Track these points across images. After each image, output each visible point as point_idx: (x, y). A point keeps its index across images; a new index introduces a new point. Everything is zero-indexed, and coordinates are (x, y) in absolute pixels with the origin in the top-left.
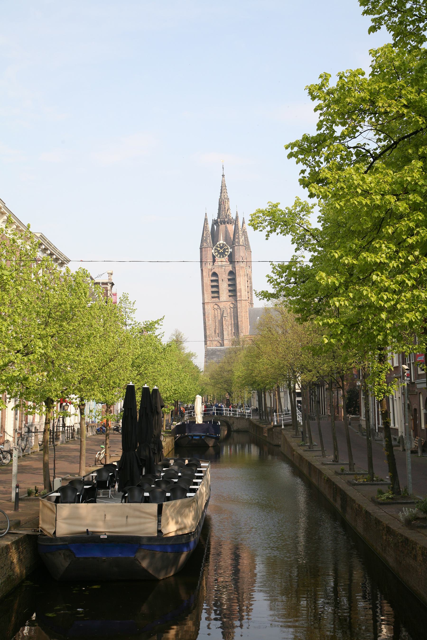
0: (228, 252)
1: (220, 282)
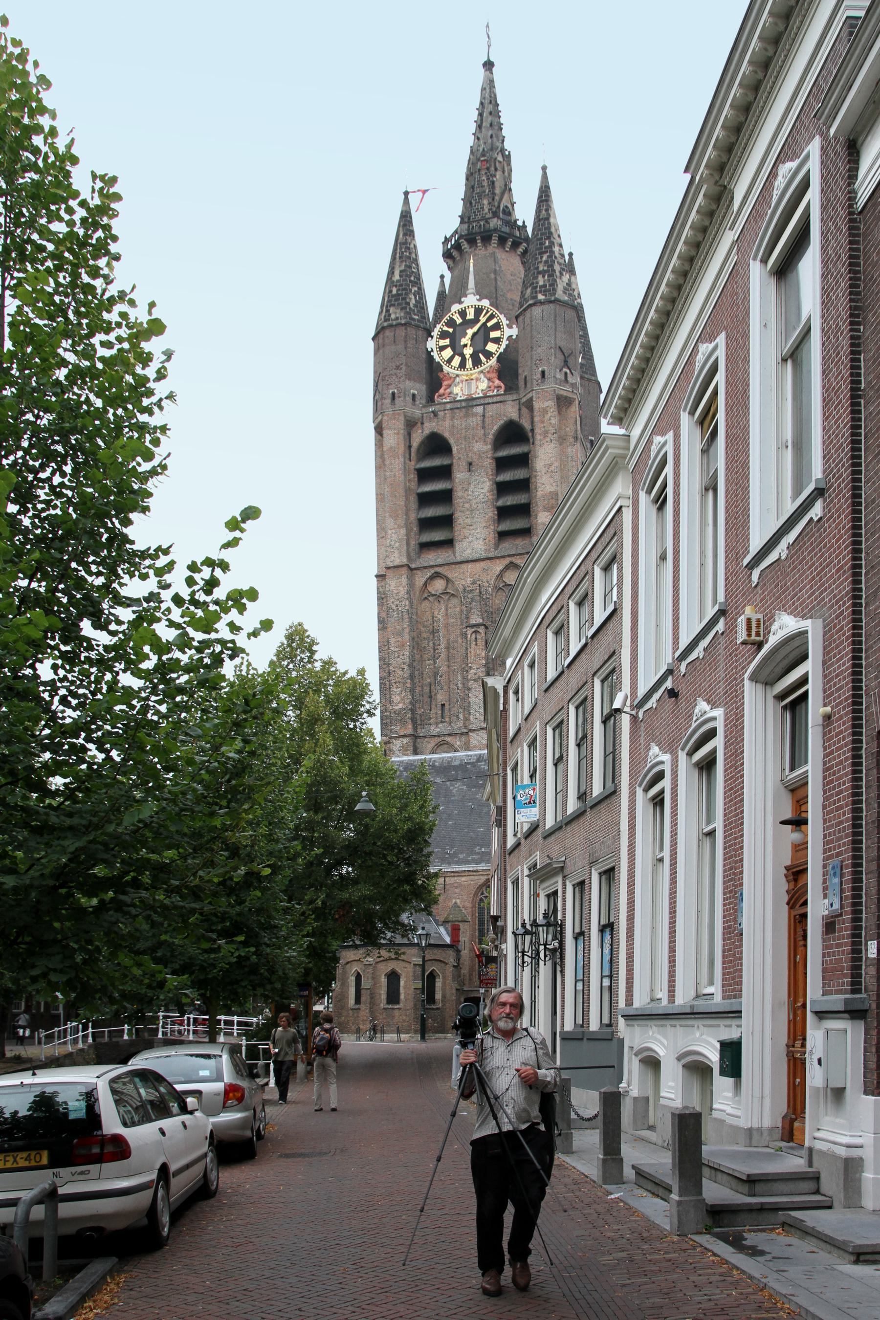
0: (497, 341)
1: (459, 475)
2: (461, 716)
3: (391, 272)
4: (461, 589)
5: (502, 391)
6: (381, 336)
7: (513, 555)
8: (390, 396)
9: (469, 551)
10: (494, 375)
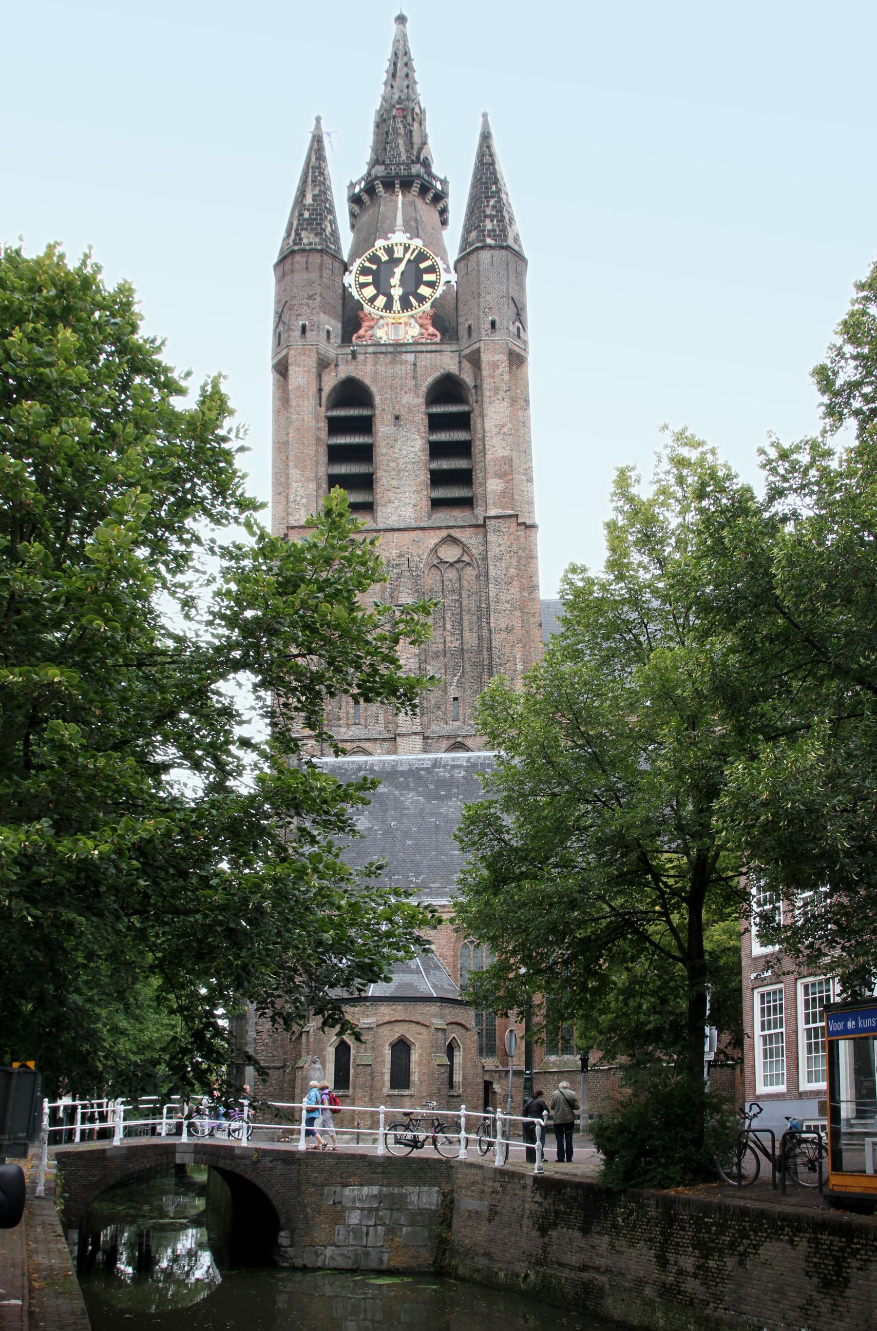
0: (432, 285)
1: (383, 428)
2: (381, 718)
3: (302, 193)
5: (438, 339)
6: (289, 261)
8: (300, 328)
9: (394, 518)
10: (428, 322)
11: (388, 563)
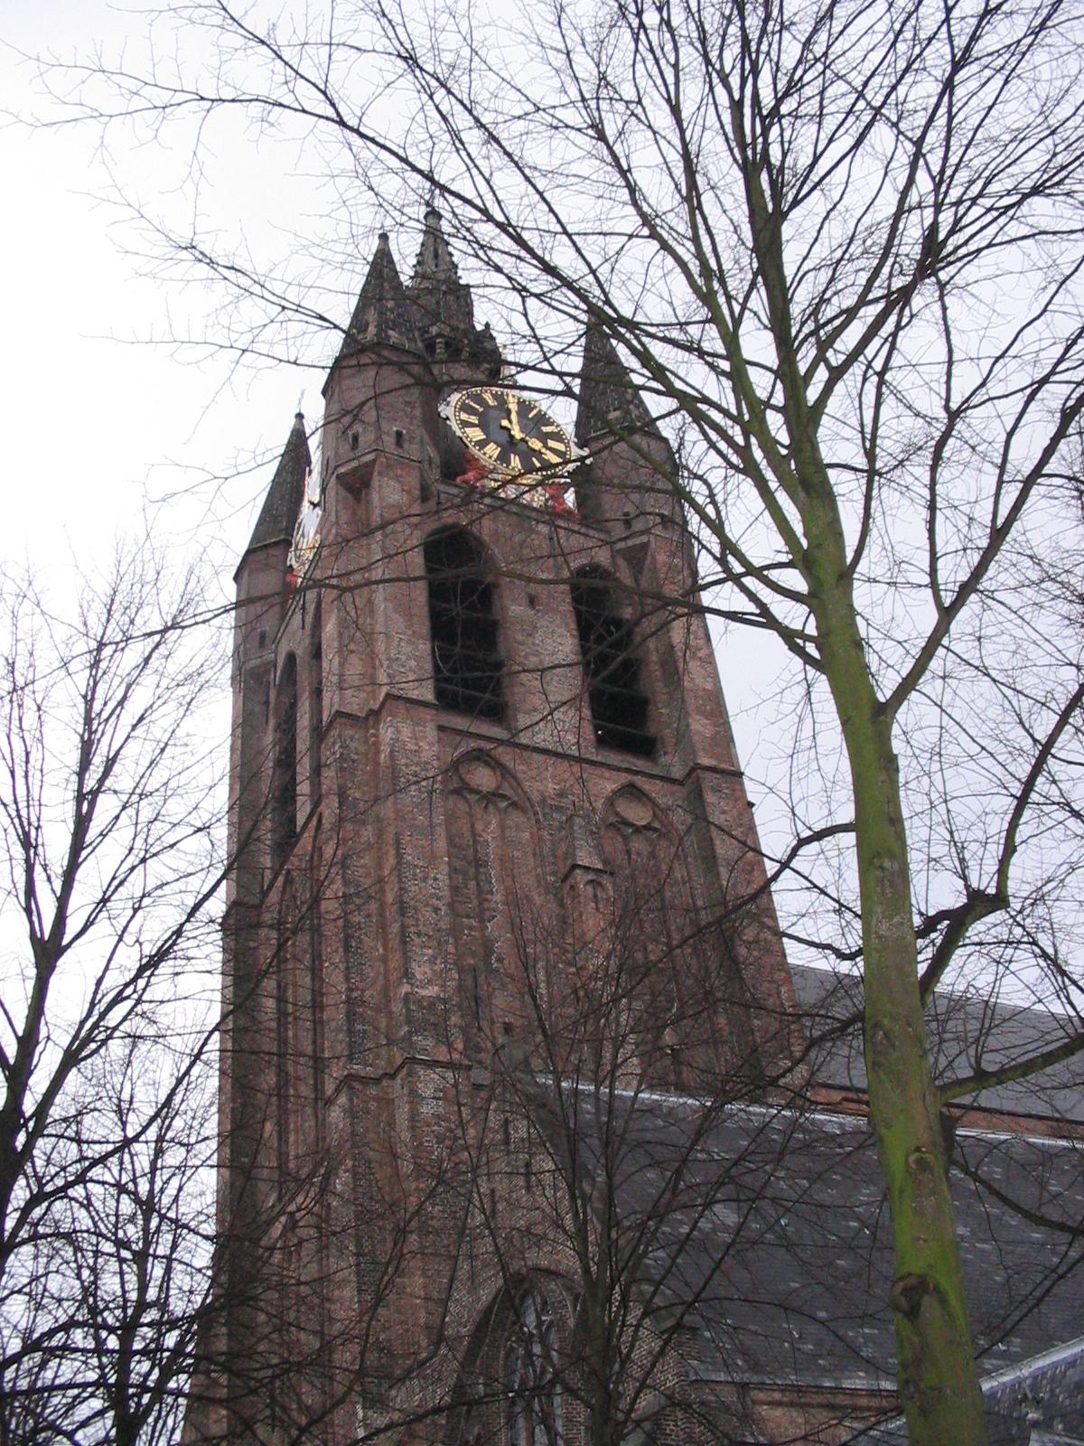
4: (535, 796)
7: (637, 773)
11: (543, 801)
